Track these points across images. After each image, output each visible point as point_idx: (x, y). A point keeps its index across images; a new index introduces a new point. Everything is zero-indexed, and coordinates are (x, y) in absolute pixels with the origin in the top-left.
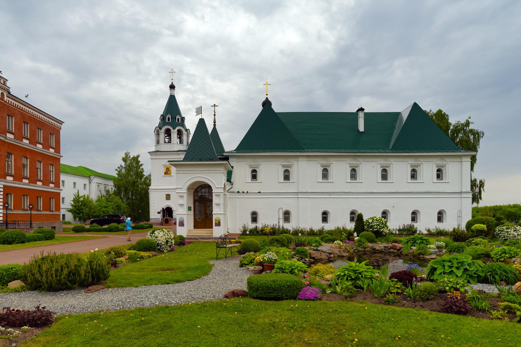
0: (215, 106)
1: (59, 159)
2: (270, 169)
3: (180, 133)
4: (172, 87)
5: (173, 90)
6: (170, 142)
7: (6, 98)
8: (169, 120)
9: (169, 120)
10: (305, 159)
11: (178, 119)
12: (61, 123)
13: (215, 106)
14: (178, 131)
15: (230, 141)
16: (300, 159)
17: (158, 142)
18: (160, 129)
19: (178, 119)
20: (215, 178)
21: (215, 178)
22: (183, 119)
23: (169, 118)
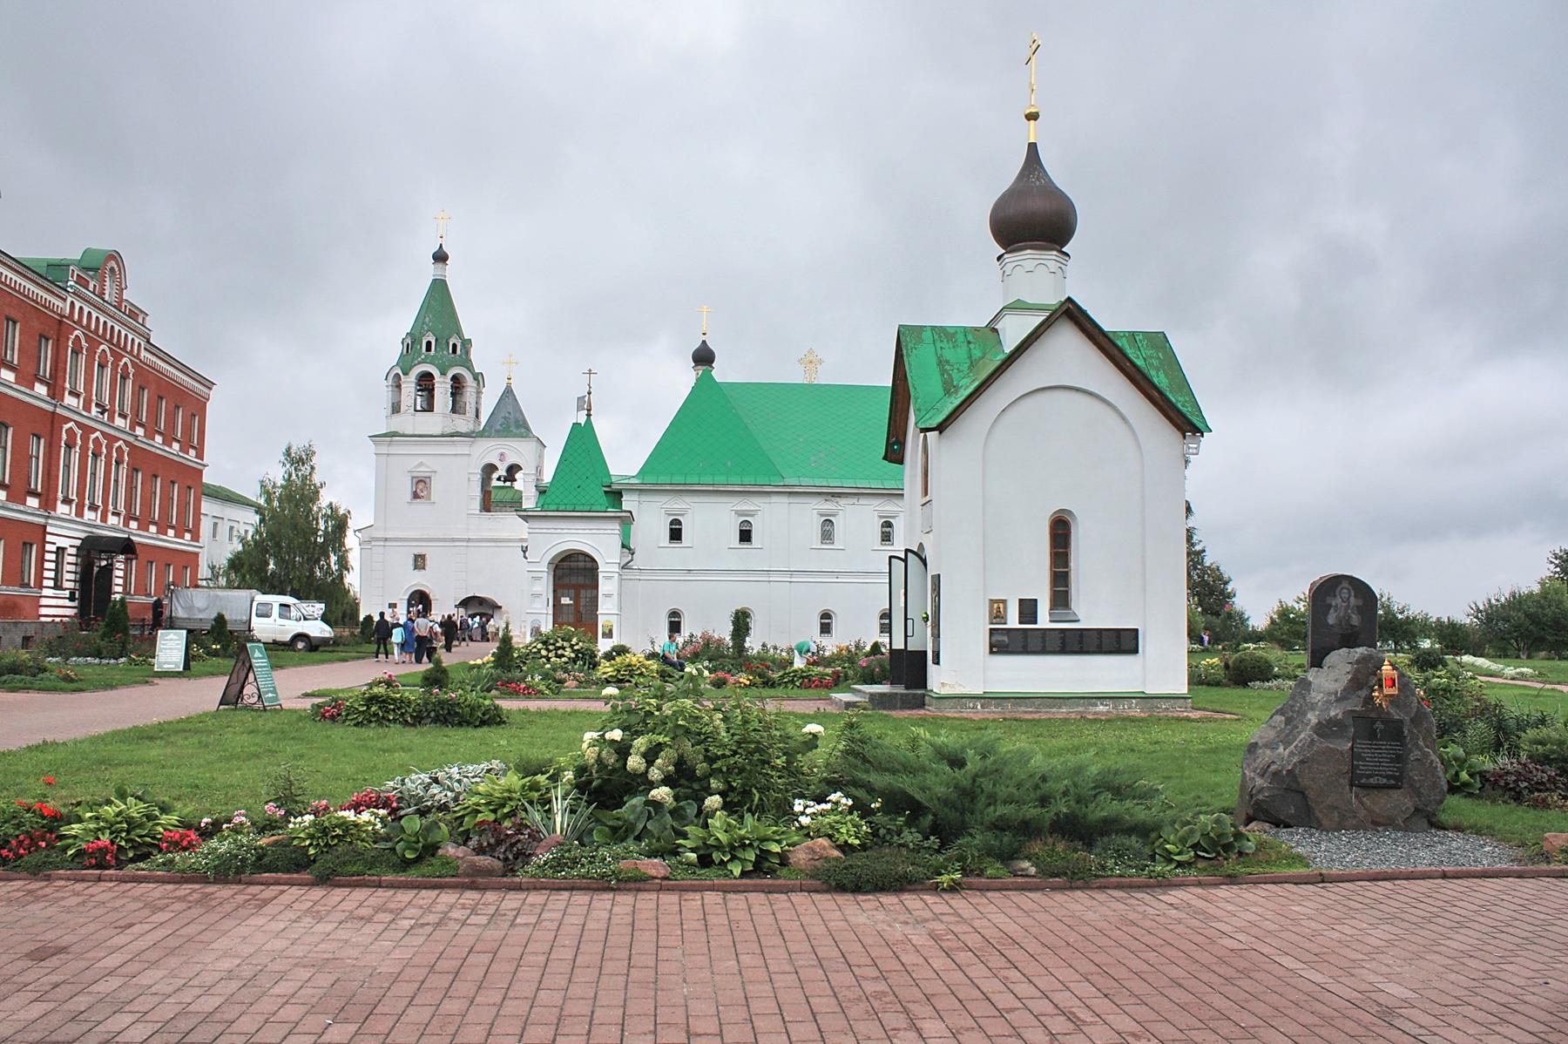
0: (590, 372)
1: (201, 472)
2: (710, 520)
3: (457, 385)
4: (440, 257)
5: (440, 265)
6: (429, 408)
7: (143, 353)
8: (429, 348)
9: (429, 348)
10: (785, 499)
11: (455, 346)
12: (209, 385)
13: (590, 372)
14: (455, 379)
15: (625, 458)
16: (774, 499)
17: (396, 409)
18: (406, 374)
19: (455, 346)
20: (599, 542)
21: (599, 542)
22: (467, 344)
23: (429, 343)
